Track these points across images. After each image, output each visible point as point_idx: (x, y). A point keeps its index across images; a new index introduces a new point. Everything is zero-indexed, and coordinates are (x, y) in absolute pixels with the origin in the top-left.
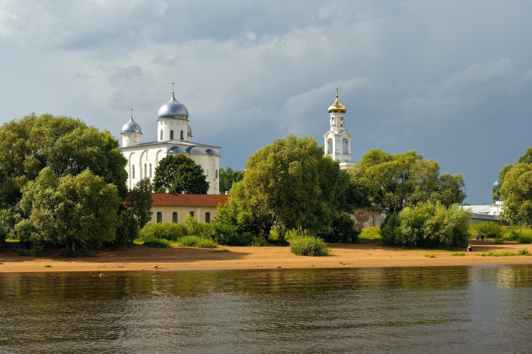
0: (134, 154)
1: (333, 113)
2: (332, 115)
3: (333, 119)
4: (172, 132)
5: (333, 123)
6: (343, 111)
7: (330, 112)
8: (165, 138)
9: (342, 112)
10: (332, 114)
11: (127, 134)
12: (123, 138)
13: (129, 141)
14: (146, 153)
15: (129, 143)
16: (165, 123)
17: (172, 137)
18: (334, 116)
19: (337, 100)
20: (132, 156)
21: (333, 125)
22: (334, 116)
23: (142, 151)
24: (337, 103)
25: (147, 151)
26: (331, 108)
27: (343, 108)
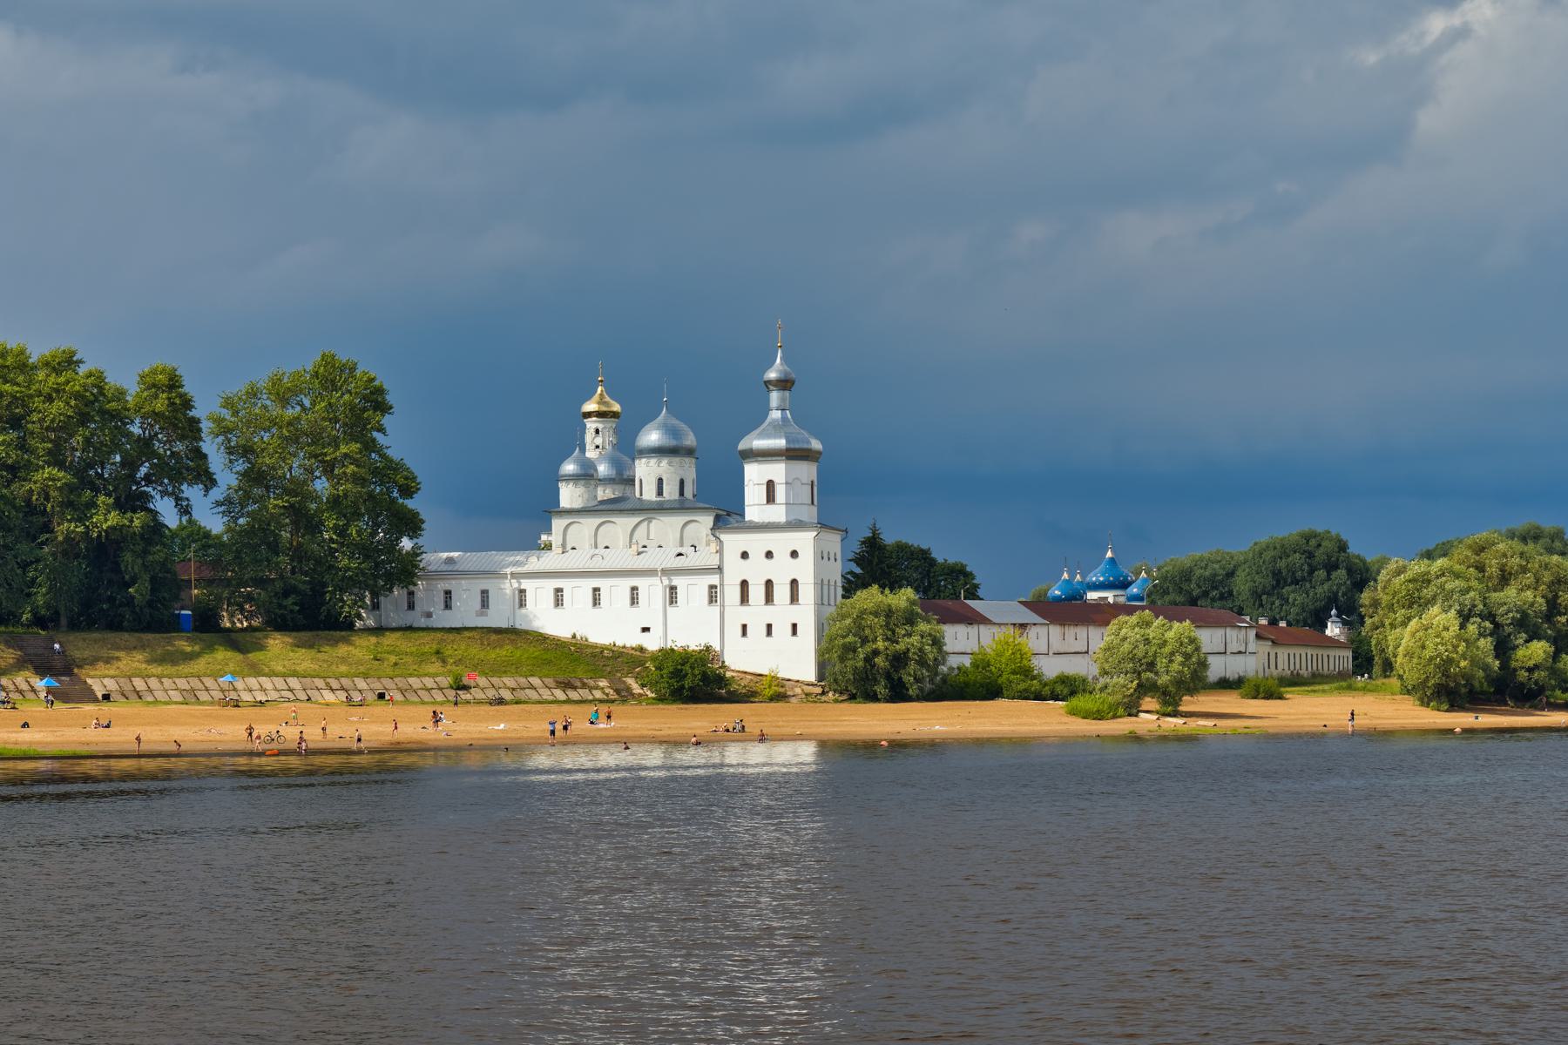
0: (607, 525)
1: (594, 419)
2: (591, 424)
3: (597, 431)
4: (682, 482)
5: (599, 441)
6: (615, 415)
7: (588, 415)
8: (670, 493)
9: (614, 417)
10: (595, 422)
11: (583, 482)
12: (561, 491)
13: (586, 496)
14: (646, 523)
15: (588, 500)
16: (670, 464)
17: (682, 493)
18: (600, 426)
19: (600, 389)
20: (601, 529)
21: (597, 447)
22: (600, 426)
23: (636, 520)
24: (601, 395)
25: (650, 520)
26: (590, 406)
27: (616, 407)
